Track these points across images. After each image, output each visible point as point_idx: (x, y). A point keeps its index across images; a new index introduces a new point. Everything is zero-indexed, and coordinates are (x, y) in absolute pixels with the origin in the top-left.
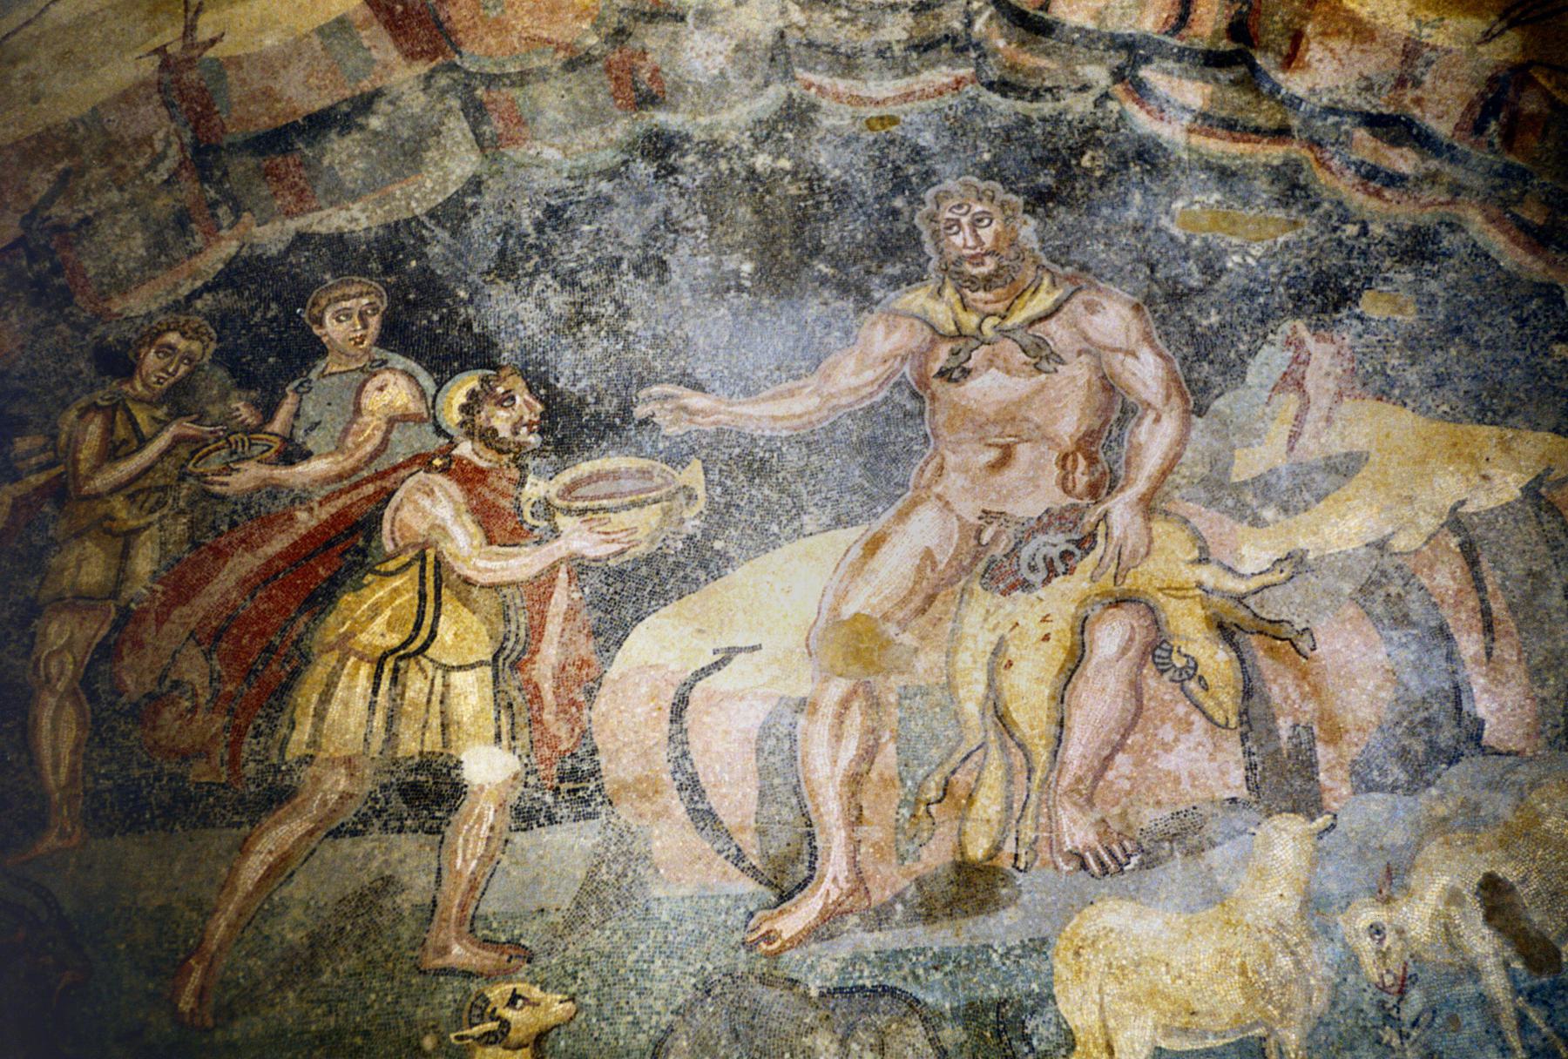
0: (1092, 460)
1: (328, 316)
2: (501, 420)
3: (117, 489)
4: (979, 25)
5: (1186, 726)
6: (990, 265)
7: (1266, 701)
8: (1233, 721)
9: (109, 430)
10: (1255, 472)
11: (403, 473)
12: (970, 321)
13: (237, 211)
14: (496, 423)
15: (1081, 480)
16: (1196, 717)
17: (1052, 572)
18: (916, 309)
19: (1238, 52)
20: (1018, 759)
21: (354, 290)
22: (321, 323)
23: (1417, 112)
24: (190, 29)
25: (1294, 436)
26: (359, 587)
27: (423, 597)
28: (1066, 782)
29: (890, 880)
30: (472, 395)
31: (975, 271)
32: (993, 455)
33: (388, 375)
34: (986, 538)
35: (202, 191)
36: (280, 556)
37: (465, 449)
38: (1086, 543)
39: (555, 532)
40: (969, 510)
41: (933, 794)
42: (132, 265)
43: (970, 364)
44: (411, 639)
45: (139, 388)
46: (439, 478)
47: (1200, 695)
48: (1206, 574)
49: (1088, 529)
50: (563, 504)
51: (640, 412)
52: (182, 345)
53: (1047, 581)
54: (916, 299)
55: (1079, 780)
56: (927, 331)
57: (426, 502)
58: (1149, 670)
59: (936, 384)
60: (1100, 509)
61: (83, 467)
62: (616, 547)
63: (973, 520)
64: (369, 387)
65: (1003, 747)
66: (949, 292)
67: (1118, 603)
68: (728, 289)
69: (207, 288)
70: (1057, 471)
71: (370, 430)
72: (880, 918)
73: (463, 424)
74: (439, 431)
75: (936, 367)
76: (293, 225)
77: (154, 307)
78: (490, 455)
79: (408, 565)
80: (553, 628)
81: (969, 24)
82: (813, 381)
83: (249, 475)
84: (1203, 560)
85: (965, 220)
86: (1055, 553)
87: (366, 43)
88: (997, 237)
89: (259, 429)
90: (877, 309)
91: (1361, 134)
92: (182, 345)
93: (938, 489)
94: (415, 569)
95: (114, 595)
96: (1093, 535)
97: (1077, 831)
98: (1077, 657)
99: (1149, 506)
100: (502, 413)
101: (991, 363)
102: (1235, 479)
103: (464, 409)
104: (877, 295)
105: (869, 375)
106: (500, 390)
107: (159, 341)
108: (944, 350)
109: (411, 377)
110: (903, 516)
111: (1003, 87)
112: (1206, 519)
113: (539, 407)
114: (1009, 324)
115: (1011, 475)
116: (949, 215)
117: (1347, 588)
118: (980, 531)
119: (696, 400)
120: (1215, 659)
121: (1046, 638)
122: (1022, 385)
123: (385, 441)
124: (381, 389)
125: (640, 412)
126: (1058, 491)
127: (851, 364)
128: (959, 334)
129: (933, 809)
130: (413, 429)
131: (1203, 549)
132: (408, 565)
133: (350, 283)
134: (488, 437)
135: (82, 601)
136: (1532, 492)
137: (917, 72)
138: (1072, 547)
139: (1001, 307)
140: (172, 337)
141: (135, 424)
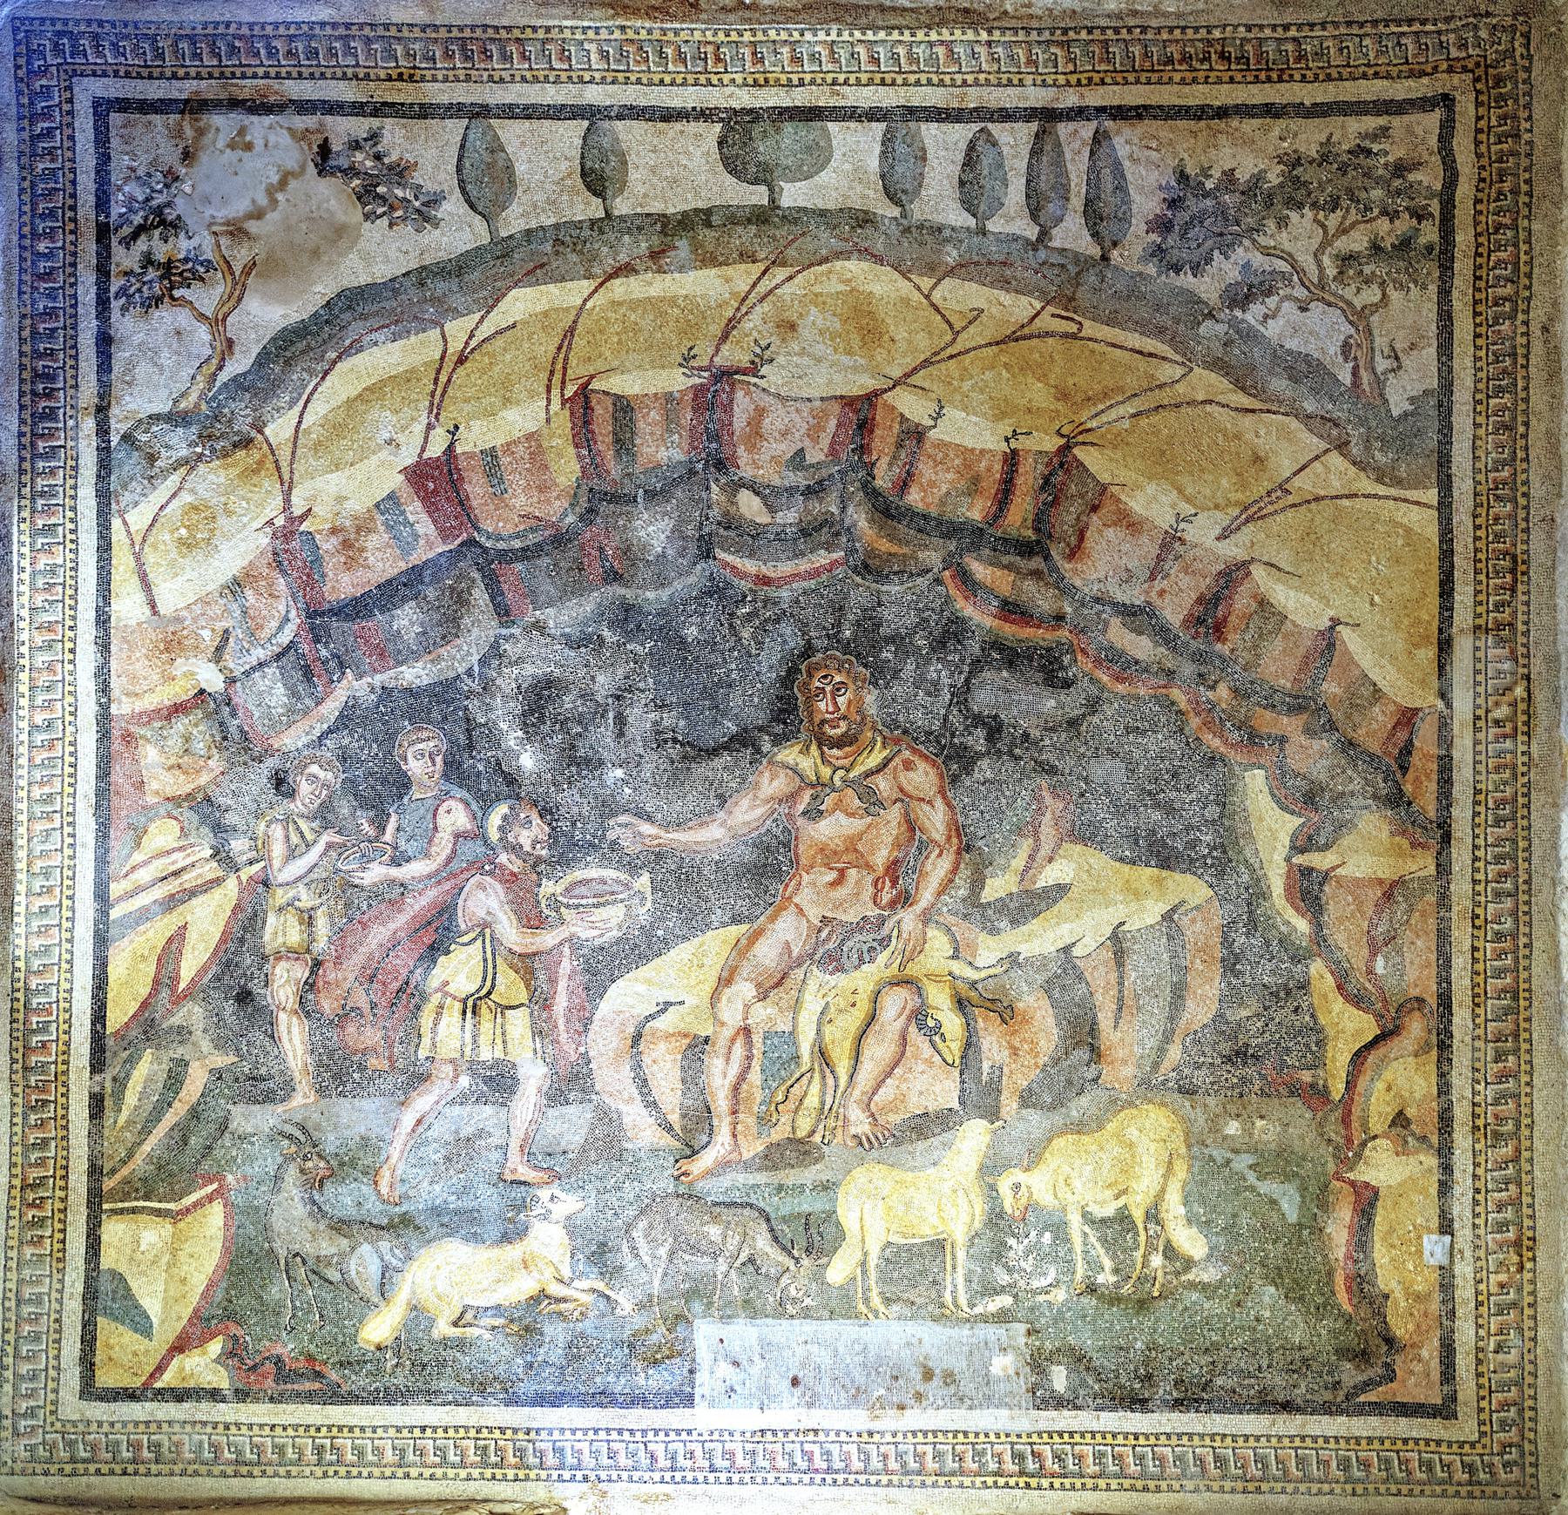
0: (894, 883)
1: (410, 756)
2: (525, 838)
3: (300, 878)
4: (850, 510)
5: (929, 1062)
6: (843, 726)
7: (979, 1051)
8: (957, 1062)
9: (287, 838)
10: (997, 896)
11: (464, 876)
12: (826, 772)
13: (342, 666)
14: (522, 840)
15: (886, 897)
16: (937, 1058)
17: (861, 961)
18: (791, 761)
19: (1038, 542)
20: (830, 1081)
21: (425, 734)
22: (405, 759)
23: (1158, 602)
24: (287, 501)
25: (1027, 869)
26: (448, 952)
27: (485, 960)
28: (857, 1093)
29: (753, 1148)
30: (505, 818)
31: (832, 732)
32: (833, 875)
33: (451, 803)
34: (824, 935)
35: (318, 651)
36: (401, 929)
37: (503, 858)
38: (884, 942)
39: (562, 922)
40: (814, 914)
41: (780, 1098)
42: (280, 710)
43: (822, 808)
44: (482, 987)
45: (299, 803)
46: (488, 878)
47: (940, 1045)
48: (958, 968)
49: (885, 931)
50: (565, 901)
51: (611, 835)
52: (321, 774)
53: (857, 967)
54: (789, 754)
55: (863, 1093)
56: (797, 779)
57: (481, 895)
58: (913, 1029)
59: (800, 822)
60: (896, 918)
61: (276, 863)
62: (596, 933)
63: (816, 922)
64: (441, 810)
65: (822, 1071)
66: (814, 747)
67: (897, 984)
68: (666, 741)
69: (330, 731)
70: (871, 890)
71: (443, 845)
72: (747, 1166)
73: (501, 839)
74: (486, 843)
75: (801, 808)
76: (378, 679)
77: (300, 744)
78: (520, 862)
79: (475, 939)
80: (562, 985)
81: (843, 509)
82: (721, 814)
83: (376, 873)
84: (955, 957)
85: (828, 689)
86: (865, 948)
87: (411, 518)
88: (850, 702)
89: (377, 839)
90: (765, 761)
91: (1116, 622)
92: (321, 774)
93: (796, 900)
94: (479, 942)
95: (308, 951)
96: (890, 937)
97: (860, 1124)
98: (872, 1018)
99: (926, 918)
100: (525, 833)
101: (838, 806)
102: (983, 901)
103: (501, 828)
104: (764, 749)
105: (759, 811)
106: (523, 815)
107: (307, 771)
108: (807, 796)
109: (467, 804)
110: (773, 919)
111: (865, 569)
112: (963, 930)
113: (547, 829)
114: (851, 775)
115: (842, 892)
116: (818, 684)
117: (1040, 979)
118: (819, 931)
119: (646, 828)
120: (952, 1024)
121: (854, 1005)
122: (858, 824)
123: (454, 851)
124: (449, 812)
125: (611, 835)
126: (871, 904)
127: (745, 802)
128: (819, 783)
129: (780, 1107)
130: (470, 844)
131: (956, 949)
132: (475, 939)
133: (421, 729)
134: (516, 849)
135: (295, 954)
136: (1168, 917)
137: (803, 554)
138: (875, 944)
139: (846, 762)
140: (314, 769)
141: (303, 837)
